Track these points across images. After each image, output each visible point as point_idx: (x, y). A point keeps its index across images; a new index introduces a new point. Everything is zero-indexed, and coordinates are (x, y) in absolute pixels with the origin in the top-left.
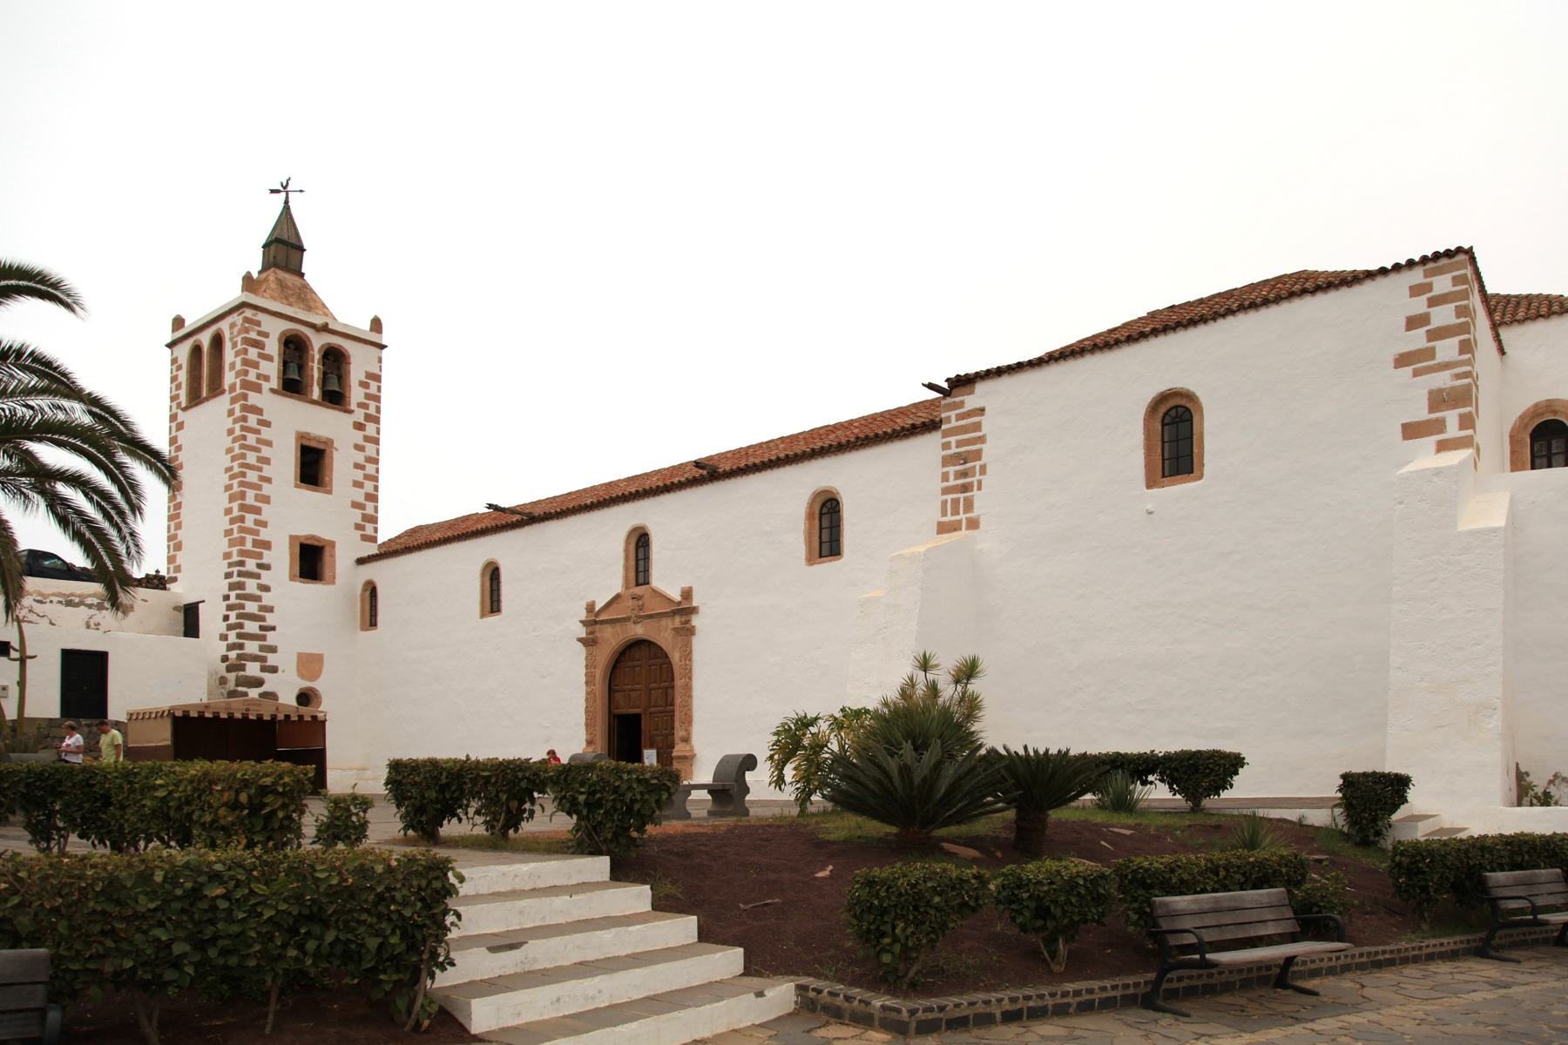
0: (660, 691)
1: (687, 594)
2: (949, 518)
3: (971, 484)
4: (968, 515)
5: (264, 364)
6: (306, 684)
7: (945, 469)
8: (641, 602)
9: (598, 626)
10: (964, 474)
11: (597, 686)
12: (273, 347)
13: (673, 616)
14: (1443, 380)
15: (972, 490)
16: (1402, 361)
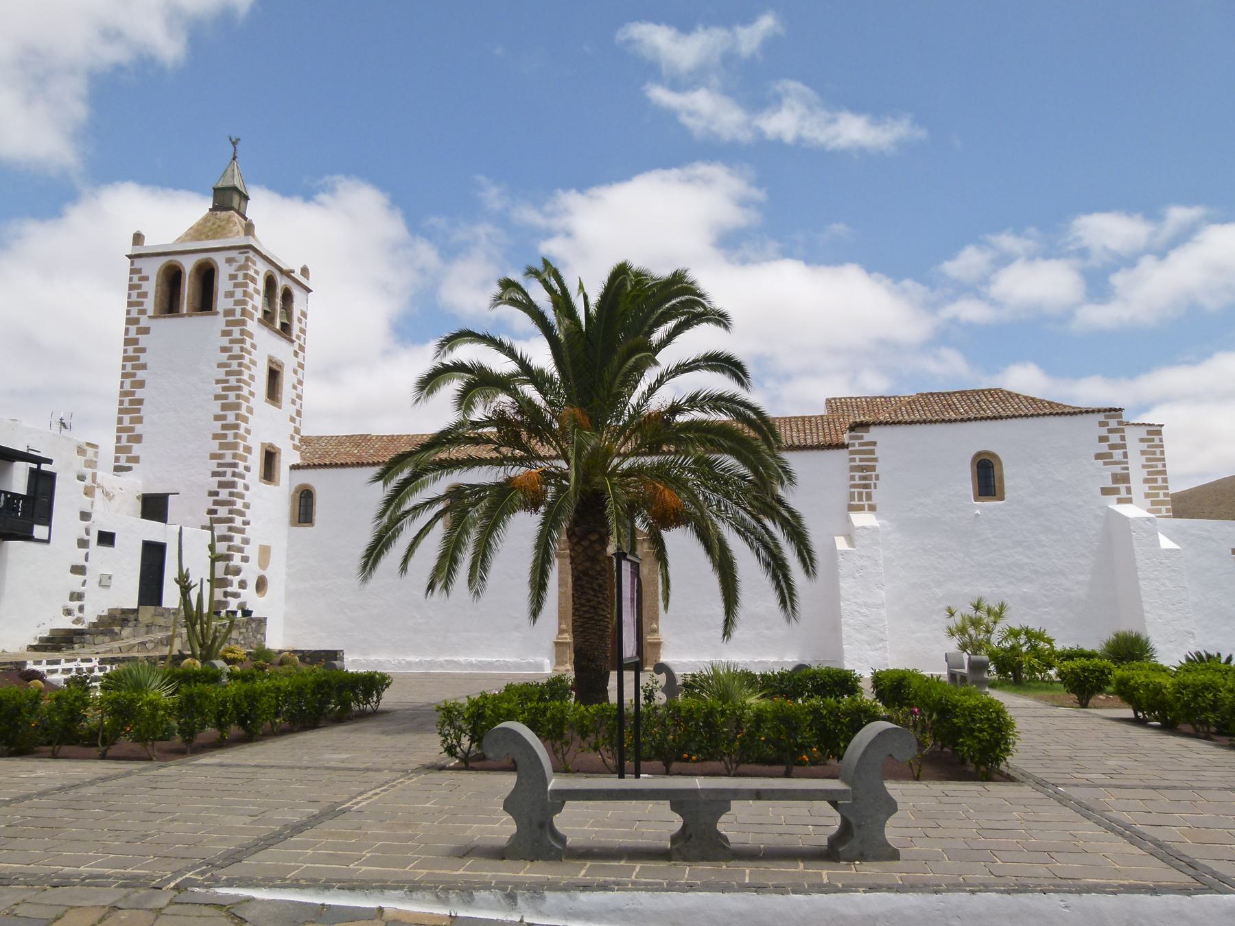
2: (856, 502)
3: (870, 484)
4: (870, 502)
5: (256, 296)
6: (262, 572)
7: (853, 474)
10: (864, 478)
15: (871, 488)
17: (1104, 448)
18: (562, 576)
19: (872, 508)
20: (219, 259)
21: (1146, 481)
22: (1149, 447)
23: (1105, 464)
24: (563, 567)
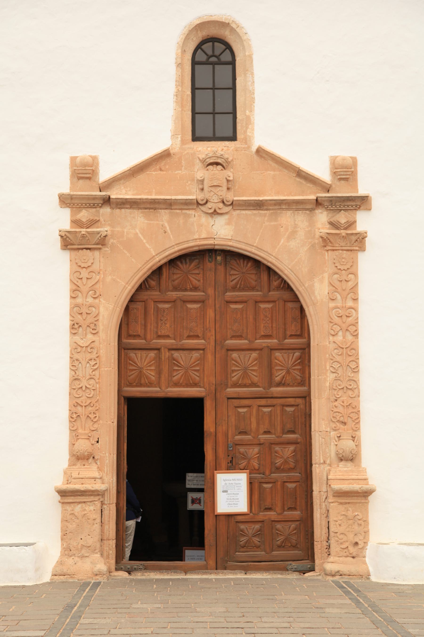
0: (254, 355)
8: (229, 173)
9: (106, 210)
11: (102, 335)
13: (312, 210)
18: (79, 300)
24: (84, 274)
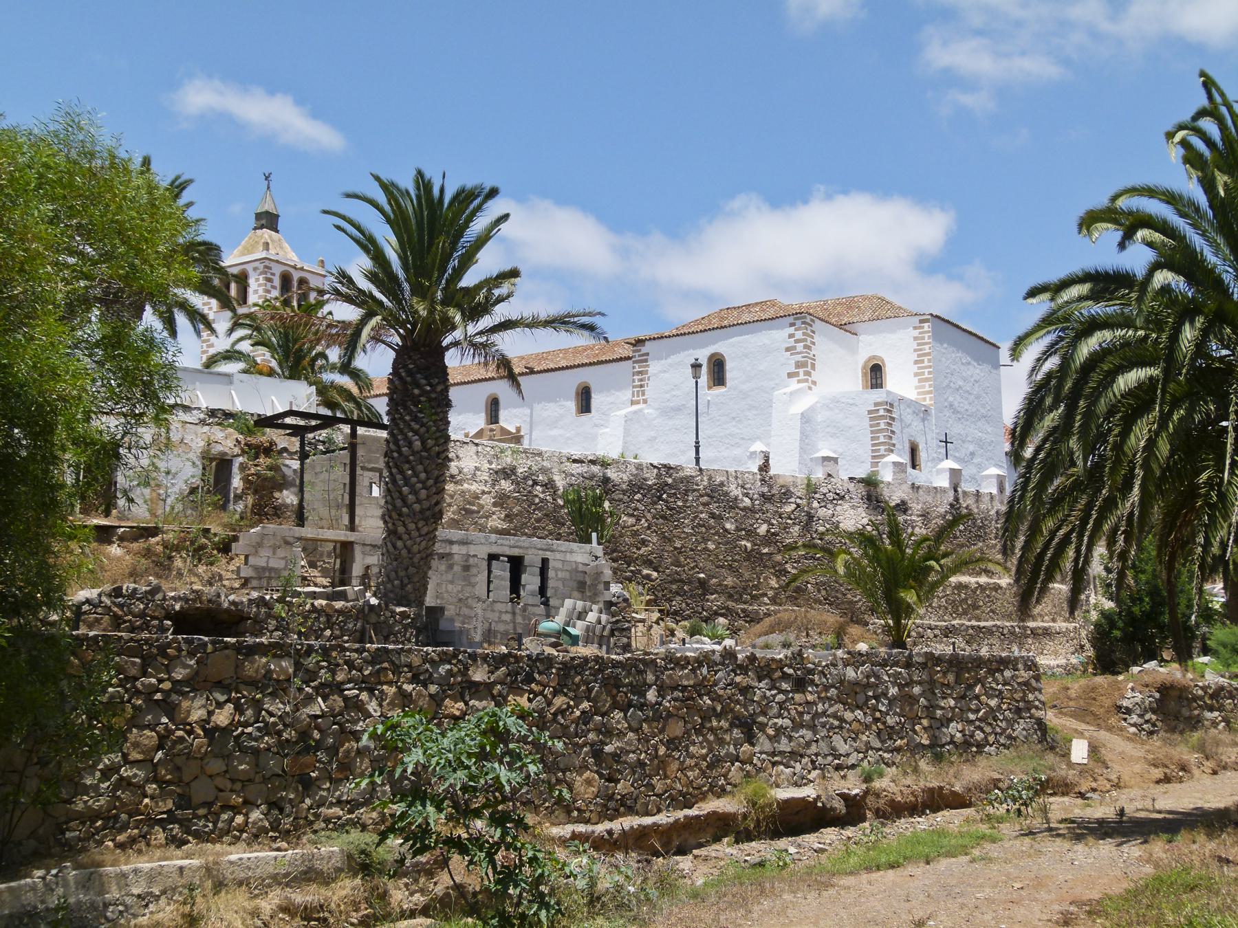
1: (518, 430)
2: (635, 398)
10: (641, 380)
12: (277, 282)
14: (799, 358)
16: (787, 349)
17: (791, 342)
19: (645, 401)
20: (249, 268)
21: (916, 362)
22: (920, 333)
23: (792, 354)
